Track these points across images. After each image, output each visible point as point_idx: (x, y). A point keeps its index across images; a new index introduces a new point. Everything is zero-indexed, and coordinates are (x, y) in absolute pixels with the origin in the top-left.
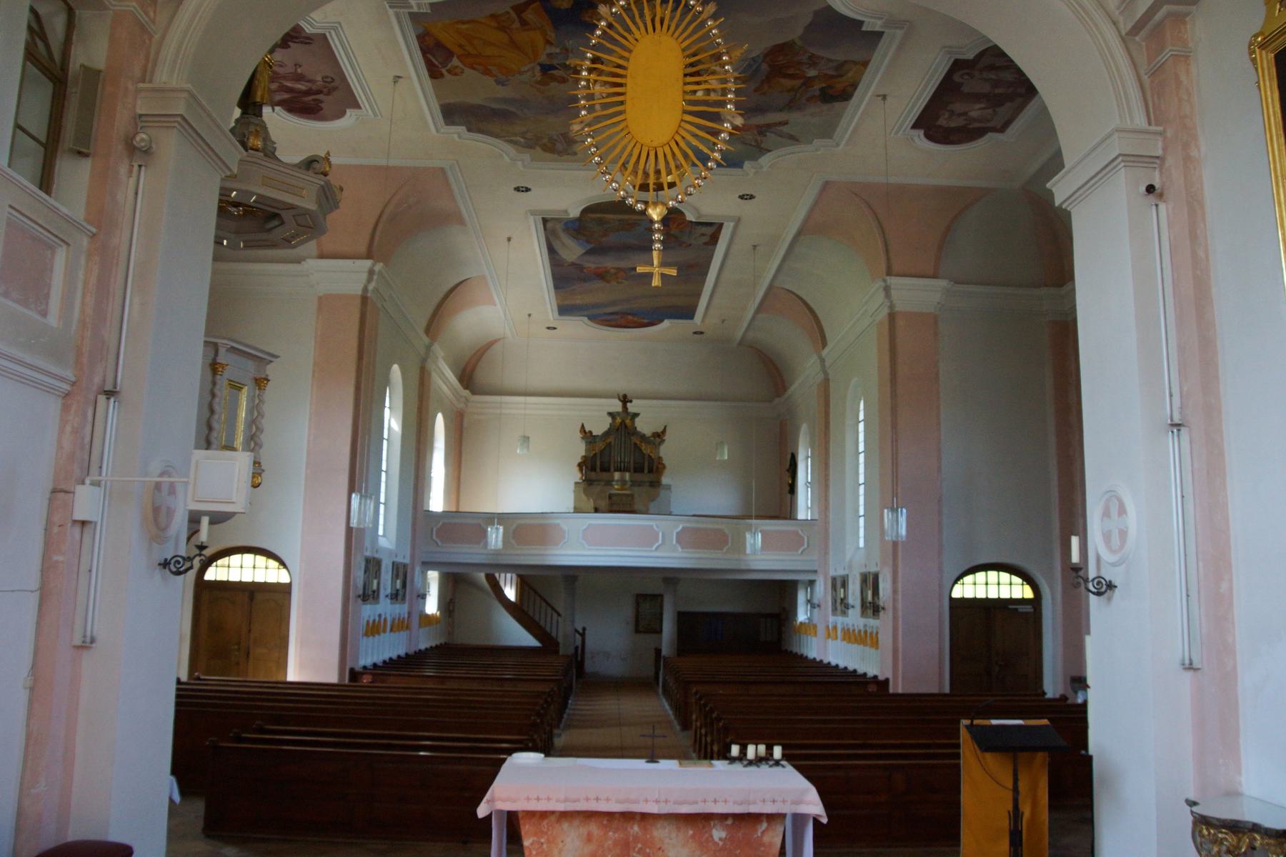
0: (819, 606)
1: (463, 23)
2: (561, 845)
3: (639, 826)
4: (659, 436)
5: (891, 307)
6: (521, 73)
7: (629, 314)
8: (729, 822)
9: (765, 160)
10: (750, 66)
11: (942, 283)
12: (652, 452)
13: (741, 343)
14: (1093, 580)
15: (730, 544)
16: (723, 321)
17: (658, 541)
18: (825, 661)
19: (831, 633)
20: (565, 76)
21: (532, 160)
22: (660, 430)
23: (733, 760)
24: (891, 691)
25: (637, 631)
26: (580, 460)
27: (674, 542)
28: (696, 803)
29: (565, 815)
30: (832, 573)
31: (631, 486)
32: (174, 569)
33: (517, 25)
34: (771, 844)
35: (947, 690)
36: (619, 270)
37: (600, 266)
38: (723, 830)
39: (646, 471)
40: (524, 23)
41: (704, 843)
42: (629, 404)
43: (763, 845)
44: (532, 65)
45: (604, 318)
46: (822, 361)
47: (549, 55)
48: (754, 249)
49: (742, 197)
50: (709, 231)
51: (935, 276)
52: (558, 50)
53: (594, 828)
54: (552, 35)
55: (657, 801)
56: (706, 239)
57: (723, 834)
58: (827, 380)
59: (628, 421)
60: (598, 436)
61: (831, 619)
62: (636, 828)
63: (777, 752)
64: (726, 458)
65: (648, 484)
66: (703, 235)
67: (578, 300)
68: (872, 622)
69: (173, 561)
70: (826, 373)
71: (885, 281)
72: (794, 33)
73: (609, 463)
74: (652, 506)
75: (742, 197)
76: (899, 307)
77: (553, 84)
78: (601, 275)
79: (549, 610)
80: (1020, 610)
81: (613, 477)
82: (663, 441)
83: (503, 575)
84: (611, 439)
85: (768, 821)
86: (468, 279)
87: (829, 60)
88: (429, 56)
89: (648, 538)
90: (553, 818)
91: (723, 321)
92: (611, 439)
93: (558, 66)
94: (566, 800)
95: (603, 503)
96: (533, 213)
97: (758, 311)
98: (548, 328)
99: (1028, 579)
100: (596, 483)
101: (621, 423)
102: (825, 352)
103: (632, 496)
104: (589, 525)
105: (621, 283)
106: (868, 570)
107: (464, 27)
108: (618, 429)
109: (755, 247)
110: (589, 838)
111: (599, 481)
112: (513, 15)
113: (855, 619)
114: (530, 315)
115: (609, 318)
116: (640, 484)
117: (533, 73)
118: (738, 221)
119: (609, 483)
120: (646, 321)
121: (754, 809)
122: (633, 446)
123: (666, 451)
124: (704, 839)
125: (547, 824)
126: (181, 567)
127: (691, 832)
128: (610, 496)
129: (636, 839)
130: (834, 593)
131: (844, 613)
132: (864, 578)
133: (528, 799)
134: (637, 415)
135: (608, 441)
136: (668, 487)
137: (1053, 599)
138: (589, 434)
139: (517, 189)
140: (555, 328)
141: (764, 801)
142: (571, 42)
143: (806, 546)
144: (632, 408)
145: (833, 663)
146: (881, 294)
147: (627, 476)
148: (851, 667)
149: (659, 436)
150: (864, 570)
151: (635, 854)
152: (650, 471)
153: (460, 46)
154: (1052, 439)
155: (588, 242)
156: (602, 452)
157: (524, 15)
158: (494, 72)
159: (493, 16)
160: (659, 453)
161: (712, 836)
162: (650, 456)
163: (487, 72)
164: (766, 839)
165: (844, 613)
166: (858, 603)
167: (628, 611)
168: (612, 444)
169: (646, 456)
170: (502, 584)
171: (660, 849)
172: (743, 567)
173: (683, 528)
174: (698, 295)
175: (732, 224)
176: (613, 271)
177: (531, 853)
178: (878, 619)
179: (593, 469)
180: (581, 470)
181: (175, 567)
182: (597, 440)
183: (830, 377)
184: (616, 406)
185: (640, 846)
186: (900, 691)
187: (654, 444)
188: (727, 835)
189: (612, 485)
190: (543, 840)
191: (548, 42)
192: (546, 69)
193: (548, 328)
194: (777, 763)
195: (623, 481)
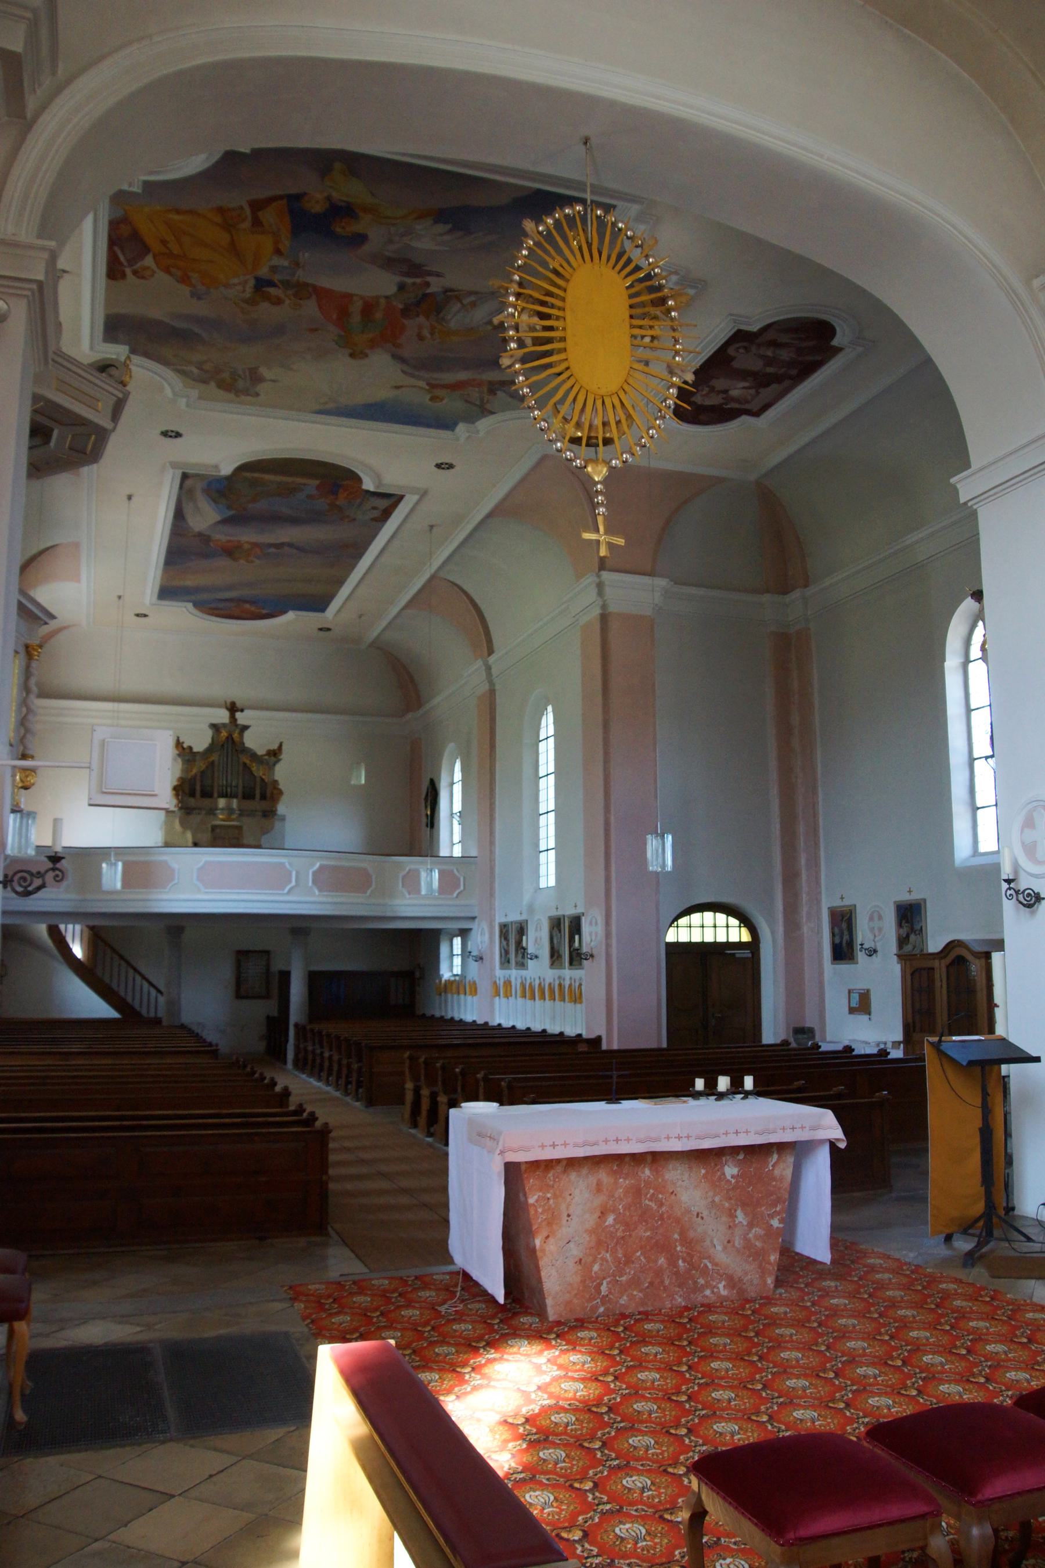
0: (481, 958)
1: (178, 212)
2: (569, 1198)
3: (650, 1170)
4: (275, 754)
5: (604, 607)
6: (227, 286)
7: (246, 602)
8: (741, 1156)
9: (484, 424)
11: (662, 582)
12: (264, 774)
13: (371, 645)
14: (1023, 892)
15: (373, 886)
16: (360, 616)
17: (290, 882)
18: (494, 1022)
19: (506, 989)
20: (282, 296)
21: (200, 398)
22: (275, 747)
23: (697, 1095)
24: (604, 1047)
25: (239, 995)
26: (175, 783)
27: (310, 883)
28: (717, 1136)
29: (572, 1163)
30: (500, 919)
31: (240, 815)
32: (20, 889)
33: (246, 225)
34: (782, 1179)
35: (664, 1045)
36: (256, 545)
37: (232, 538)
38: (735, 1166)
39: (258, 796)
40: (257, 223)
41: (716, 1182)
42: (238, 715)
43: (774, 1179)
45: (213, 605)
46: (488, 668)
47: (274, 269)
48: (431, 530)
49: (439, 466)
50: (383, 504)
51: (651, 574)
52: (286, 263)
53: (603, 1175)
54: (286, 243)
55: (679, 1138)
56: (376, 514)
57: (735, 1171)
58: (492, 692)
59: (236, 736)
60: (198, 753)
61: (500, 974)
62: (647, 1172)
63: (749, 1082)
64: (363, 782)
65: (260, 814)
66: (374, 508)
67: (190, 582)
68: (568, 974)
69: (16, 878)
70: (491, 683)
71: (599, 576)
73: (212, 786)
74: (264, 840)
75: (439, 466)
76: (612, 608)
77: (265, 305)
78: (230, 551)
79: (131, 972)
80: (737, 956)
81: (216, 803)
82: (279, 760)
83: (70, 927)
84: (214, 757)
85: (779, 1153)
86: (57, 545)
88: (116, 248)
89: (278, 879)
90: (559, 1169)
91: (360, 616)
92: (214, 757)
94: (585, 1144)
95: (207, 836)
96: (174, 465)
97: (407, 606)
98: (138, 615)
99: (745, 921)
100: (197, 811)
101: (227, 738)
102: (492, 659)
103: (239, 828)
104: (207, 863)
105: (252, 562)
106: (560, 913)
107: (177, 217)
108: (223, 745)
109: (432, 527)
110: (599, 1188)
111: (200, 809)
112: (248, 211)
113: (539, 970)
114: (120, 597)
115: (221, 605)
116: (251, 814)
118: (424, 494)
119: (212, 811)
120: (264, 612)
121: (774, 1139)
122: (241, 768)
123: (281, 773)
124: (715, 1179)
125: (553, 1176)
126: (30, 885)
127: (703, 1171)
128: (214, 828)
129: (648, 1184)
130: (504, 943)
131: (522, 965)
132: (556, 924)
133: (543, 1146)
134: (246, 728)
135: (211, 760)
136: (283, 819)
137: (774, 941)
138: (188, 751)
139: (165, 434)
140: (145, 616)
141: (784, 1129)
142: (306, 255)
143: (462, 888)
144: (241, 718)
145: (507, 1023)
146: (593, 593)
147: (235, 803)
148: (537, 1027)
149: (275, 754)
150: (554, 913)
151: (647, 1202)
152: (263, 797)
153: (164, 242)
154: (773, 764)
155: (229, 508)
156: (203, 773)
157: (260, 214)
159: (221, 210)
160: (273, 774)
161: (724, 1174)
162: (262, 780)
163: (185, 280)
164: (777, 1172)
165: (522, 965)
166: (545, 952)
167: (226, 972)
168: (216, 763)
169: (258, 780)
170: (69, 939)
171: (672, 1193)
172: (389, 914)
173: (322, 868)
174: (340, 582)
175: (416, 498)
176: (246, 546)
177: (536, 1211)
178: (583, 969)
179: (192, 794)
180: (177, 795)
181: (21, 885)
182: (198, 758)
183: (497, 687)
184: (222, 716)
185: (652, 1191)
186: (615, 1047)
187: (268, 764)
188: (739, 1171)
189: (215, 815)
190: (549, 1195)
191: (278, 252)
192: (261, 284)
193: (138, 615)
194: (747, 1094)
195: (229, 810)
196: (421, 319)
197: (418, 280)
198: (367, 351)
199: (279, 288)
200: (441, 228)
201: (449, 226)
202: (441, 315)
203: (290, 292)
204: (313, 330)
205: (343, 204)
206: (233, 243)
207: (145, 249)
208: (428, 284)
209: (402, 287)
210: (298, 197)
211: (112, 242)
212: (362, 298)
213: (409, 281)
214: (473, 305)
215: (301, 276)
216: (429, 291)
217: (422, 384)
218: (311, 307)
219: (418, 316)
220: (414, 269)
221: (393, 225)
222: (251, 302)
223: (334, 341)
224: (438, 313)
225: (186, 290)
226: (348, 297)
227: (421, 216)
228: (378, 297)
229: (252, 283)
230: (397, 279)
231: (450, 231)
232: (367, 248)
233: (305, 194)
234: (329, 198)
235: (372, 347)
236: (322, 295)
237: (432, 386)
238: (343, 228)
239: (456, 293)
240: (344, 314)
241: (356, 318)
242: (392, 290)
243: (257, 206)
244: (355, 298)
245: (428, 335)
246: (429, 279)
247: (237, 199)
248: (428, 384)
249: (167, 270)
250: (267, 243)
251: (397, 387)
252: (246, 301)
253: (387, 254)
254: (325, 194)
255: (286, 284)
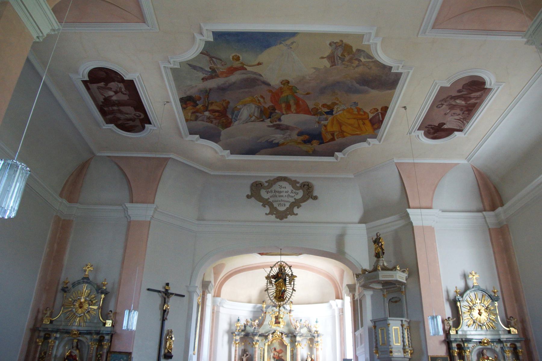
1: (357, 134)
6: (344, 110)
10: (237, 116)
20: (322, 108)
33: (336, 134)
40: (333, 134)
44: (336, 114)
52: (322, 122)
54: (323, 129)
72: (224, 132)
77: (329, 103)
87: (203, 120)
88: (381, 119)
93: (324, 114)
107: (358, 133)
117: (337, 110)
142: (316, 127)
153: (364, 124)
157: (332, 137)
158: (356, 110)
159: (344, 137)
163: (359, 110)
191: (325, 126)
192: (330, 113)
196: (267, 106)
197: (275, 123)
198: (282, 86)
199: (324, 112)
200: (276, 141)
201: (274, 142)
202: (260, 109)
203: (320, 111)
204: (308, 94)
205: (307, 144)
206: (341, 126)
207: (371, 121)
208: (271, 122)
209: (280, 120)
210: (321, 143)
211: (382, 122)
212: (292, 113)
213: (278, 123)
214: (250, 116)
215: (315, 118)
216: (269, 119)
217: (249, 69)
218: (311, 105)
219: (268, 108)
220: (279, 127)
221: (291, 140)
222: (335, 104)
223: (298, 89)
224: (261, 110)
225: (360, 106)
226: (297, 113)
227: (283, 144)
228: (287, 114)
229: (334, 113)
230: (282, 123)
231: (272, 141)
232: (296, 132)
233: (319, 144)
234: (312, 145)
235: (281, 88)
236: (307, 111)
237: (242, 68)
238: (305, 137)
239: (259, 120)
240: (297, 104)
241: (292, 102)
242: (283, 118)
243: (333, 139)
244: (295, 112)
245: (260, 99)
246: (272, 124)
247: (338, 141)
248: (245, 69)
249: (365, 112)
250: (329, 129)
251: (259, 64)
252: (337, 104)
253: (289, 131)
254: (313, 145)
255: (321, 114)
